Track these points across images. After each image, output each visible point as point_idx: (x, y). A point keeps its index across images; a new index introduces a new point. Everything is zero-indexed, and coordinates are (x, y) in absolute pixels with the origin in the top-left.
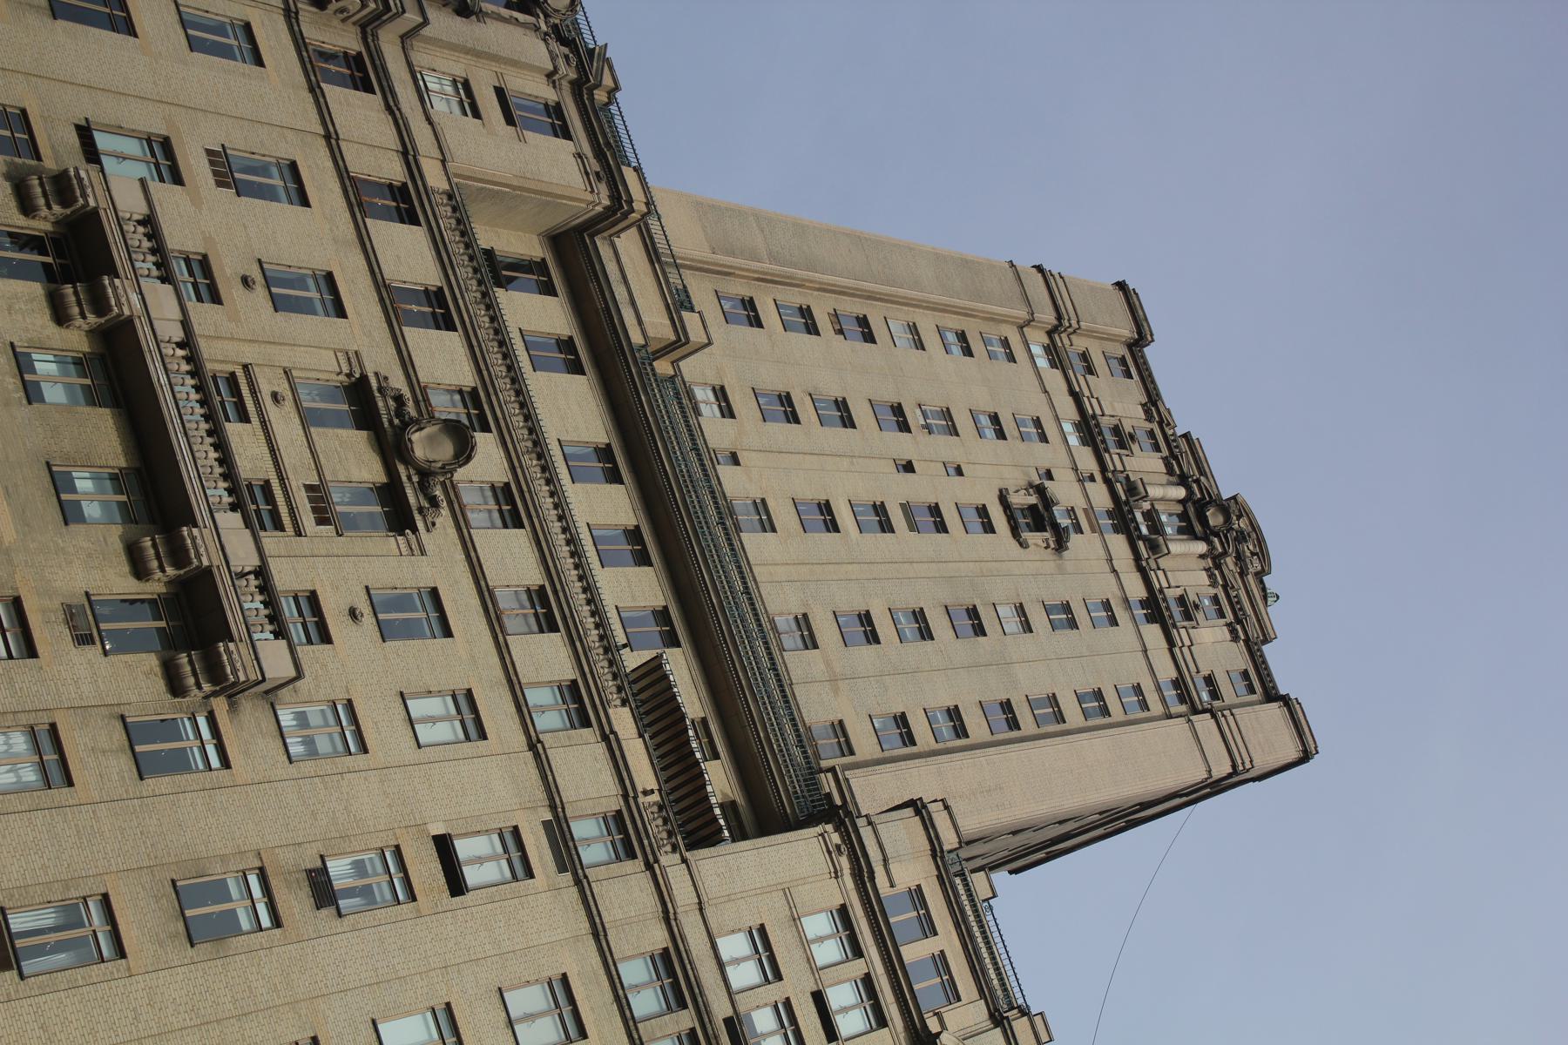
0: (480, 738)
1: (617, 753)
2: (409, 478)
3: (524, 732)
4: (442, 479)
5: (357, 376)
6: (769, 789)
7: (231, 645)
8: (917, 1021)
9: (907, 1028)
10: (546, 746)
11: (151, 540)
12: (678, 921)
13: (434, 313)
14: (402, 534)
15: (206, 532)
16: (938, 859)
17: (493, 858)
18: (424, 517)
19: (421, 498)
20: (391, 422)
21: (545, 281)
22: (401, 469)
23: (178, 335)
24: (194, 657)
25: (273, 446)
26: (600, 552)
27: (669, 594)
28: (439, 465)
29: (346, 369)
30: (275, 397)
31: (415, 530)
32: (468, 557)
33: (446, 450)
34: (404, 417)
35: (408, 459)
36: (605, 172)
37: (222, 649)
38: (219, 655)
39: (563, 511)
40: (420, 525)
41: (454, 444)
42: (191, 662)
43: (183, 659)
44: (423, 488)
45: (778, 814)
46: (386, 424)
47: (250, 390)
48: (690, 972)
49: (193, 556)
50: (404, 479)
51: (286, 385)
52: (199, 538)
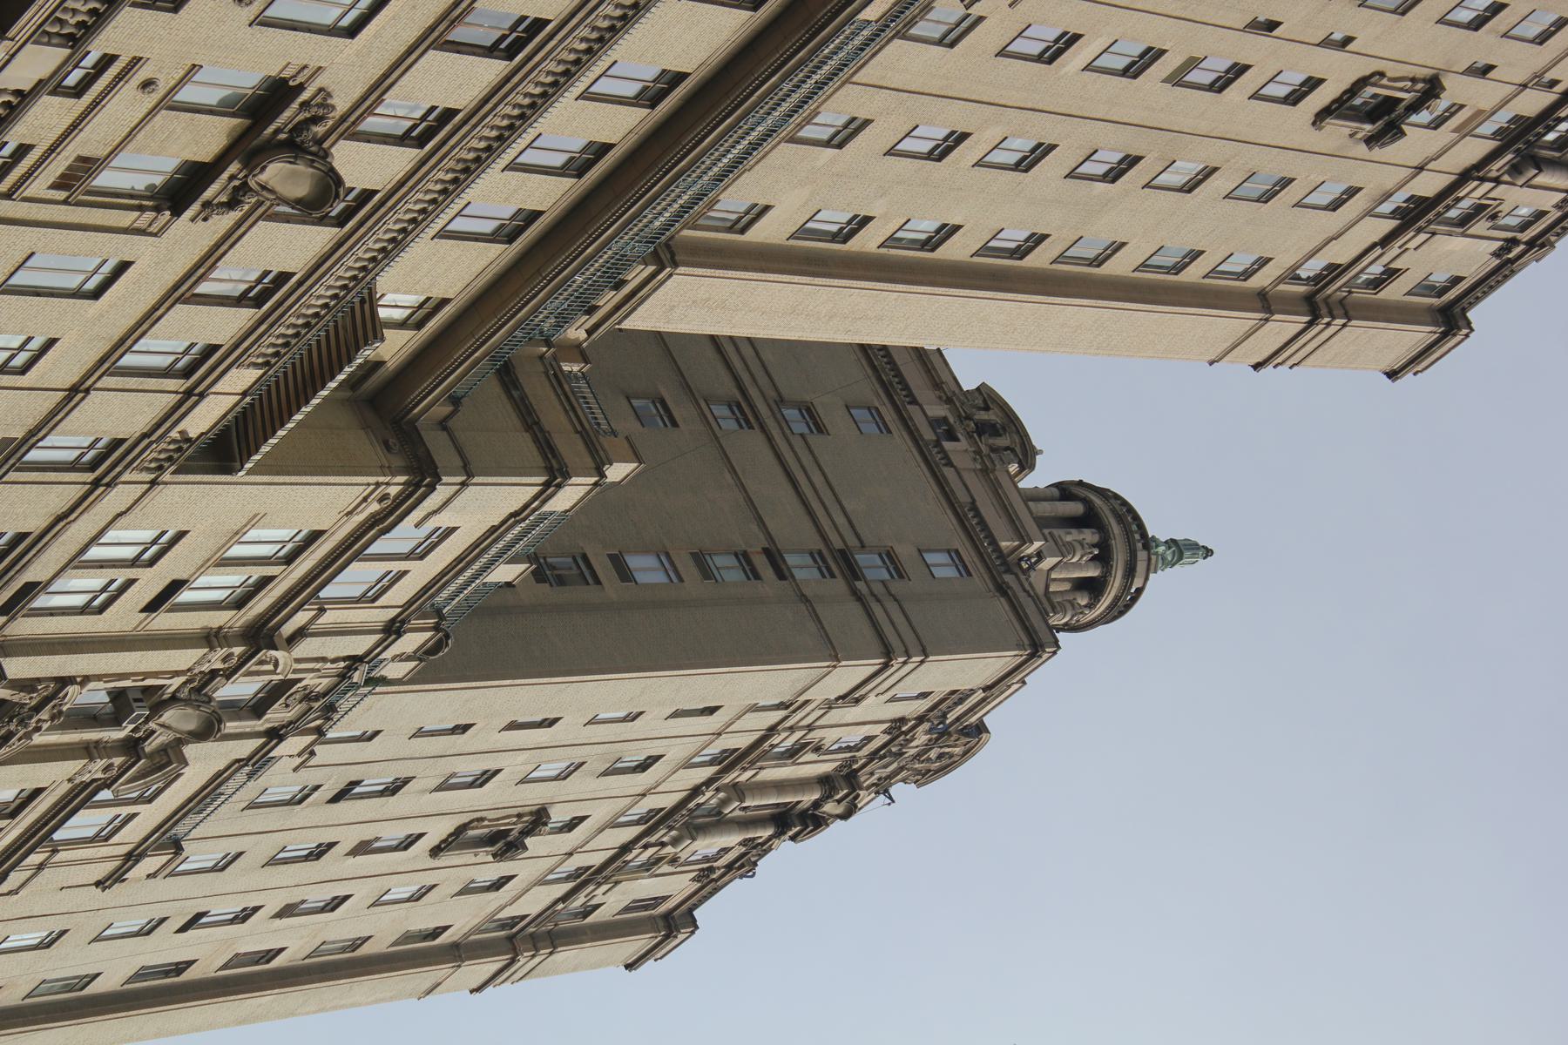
1: (183, 410)
2: (232, 178)
3: (84, 376)
5: (291, 83)
8: (274, 621)
9: (262, 615)
12: (68, 526)
22: (234, 168)
25: (79, 124)
31: (177, 212)
32: (217, 246)
34: (298, 136)
36: (392, 504)
39: (424, 220)
40: (189, 213)
41: (308, 194)
45: (406, 403)
48: (12, 573)
50: (225, 175)
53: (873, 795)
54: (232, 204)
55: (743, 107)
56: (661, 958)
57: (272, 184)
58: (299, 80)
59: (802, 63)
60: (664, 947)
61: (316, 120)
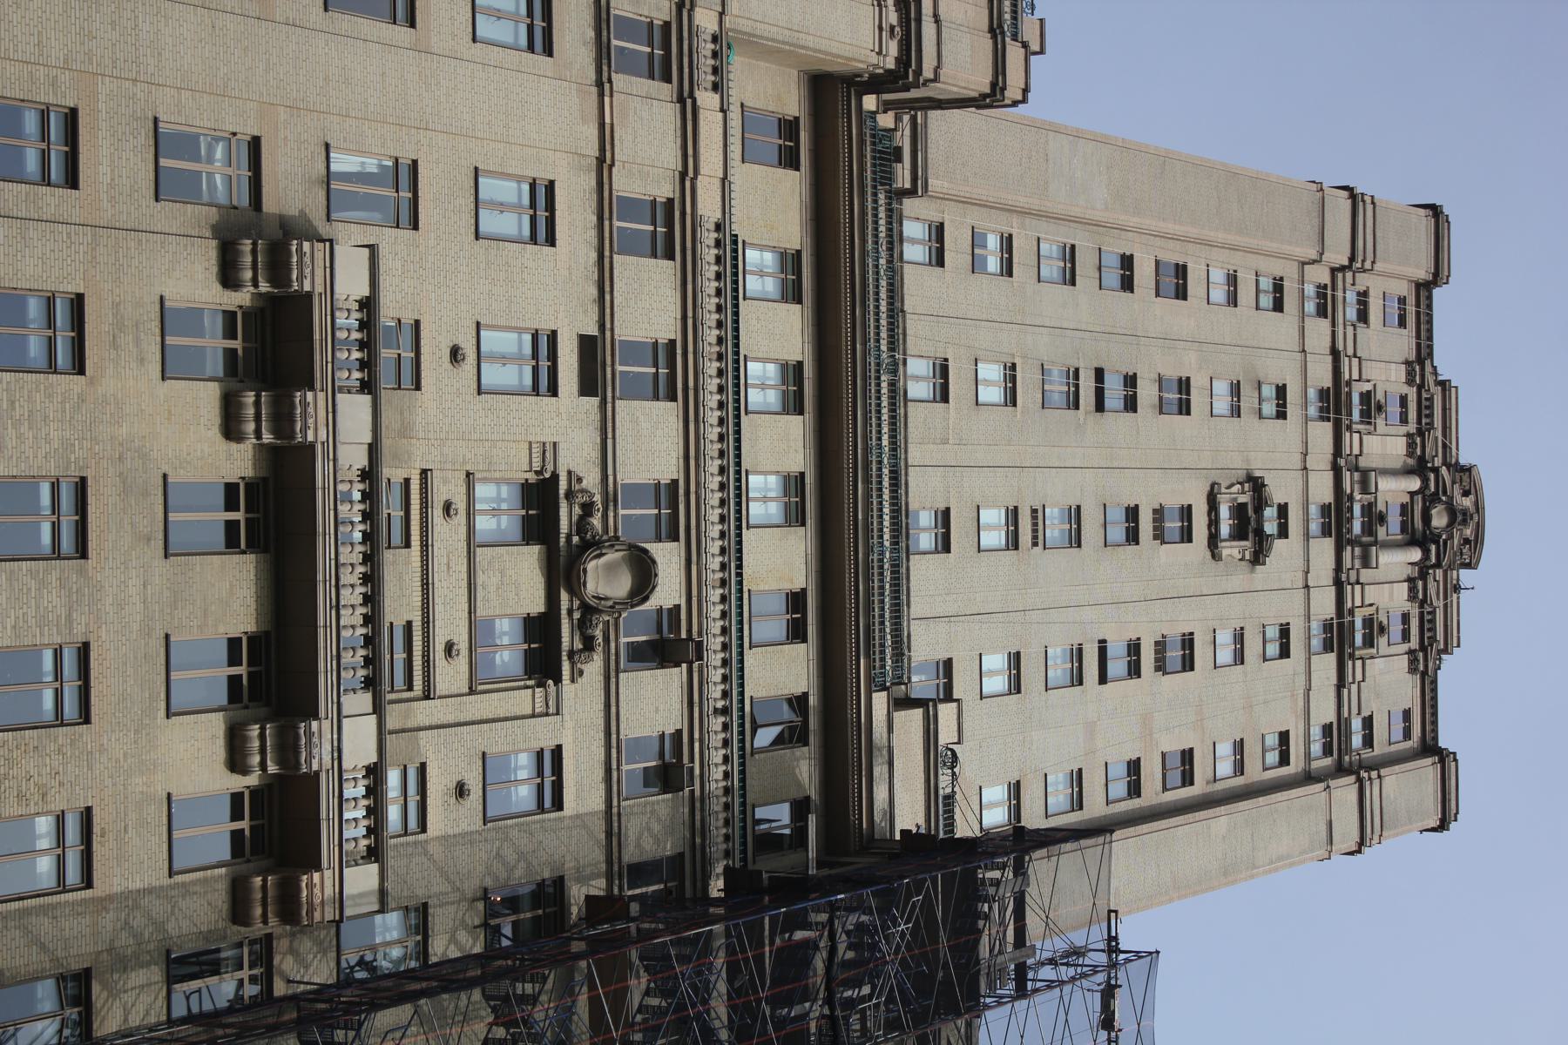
0: (544, 52)
2: (570, 612)
4: (607, 618)
5: (547, 475)
6: (846, 519)
7: (310, 395)
10: (615, 88)
11: (255, 396)
13: (651, 55)
14: (541, 684)
15: (321, 395)
16: (1000, 85)
17: (517, 359)
18: (573, 664)
19: (577, 638)
20: (569, 537)
21: (791, 147)
22: (564, 596)
23: (362, 461)
24: (263, 399)
26: (746, 140)
27: (814, 680)
28: (610, 603)
29: (537, 466)
30: (447, 508)
31: (558, 680)
33: (621, 586)
34: (586, 534)
35: (575, 588)
37: (294, 248)
38: (297, 737)
42: (257, 404)
43: (249, 398)
44: (583, 626)
46: (562, 540)
47: (421, 504)
49: (294, 277)
50: (564, 612)
51: (465, 637)
52: (311, 405)
53: (1455, 596)
54: (589, 644)
55: (864, 767)
56: (1457, 813)
57: (603, 590)
58: (550, 467)
59: (867, 496)
60: (1450, 789)
61: (588, 508)
